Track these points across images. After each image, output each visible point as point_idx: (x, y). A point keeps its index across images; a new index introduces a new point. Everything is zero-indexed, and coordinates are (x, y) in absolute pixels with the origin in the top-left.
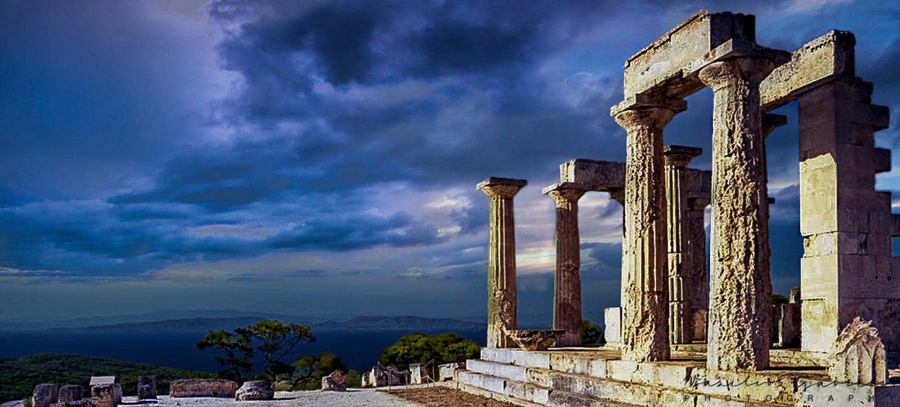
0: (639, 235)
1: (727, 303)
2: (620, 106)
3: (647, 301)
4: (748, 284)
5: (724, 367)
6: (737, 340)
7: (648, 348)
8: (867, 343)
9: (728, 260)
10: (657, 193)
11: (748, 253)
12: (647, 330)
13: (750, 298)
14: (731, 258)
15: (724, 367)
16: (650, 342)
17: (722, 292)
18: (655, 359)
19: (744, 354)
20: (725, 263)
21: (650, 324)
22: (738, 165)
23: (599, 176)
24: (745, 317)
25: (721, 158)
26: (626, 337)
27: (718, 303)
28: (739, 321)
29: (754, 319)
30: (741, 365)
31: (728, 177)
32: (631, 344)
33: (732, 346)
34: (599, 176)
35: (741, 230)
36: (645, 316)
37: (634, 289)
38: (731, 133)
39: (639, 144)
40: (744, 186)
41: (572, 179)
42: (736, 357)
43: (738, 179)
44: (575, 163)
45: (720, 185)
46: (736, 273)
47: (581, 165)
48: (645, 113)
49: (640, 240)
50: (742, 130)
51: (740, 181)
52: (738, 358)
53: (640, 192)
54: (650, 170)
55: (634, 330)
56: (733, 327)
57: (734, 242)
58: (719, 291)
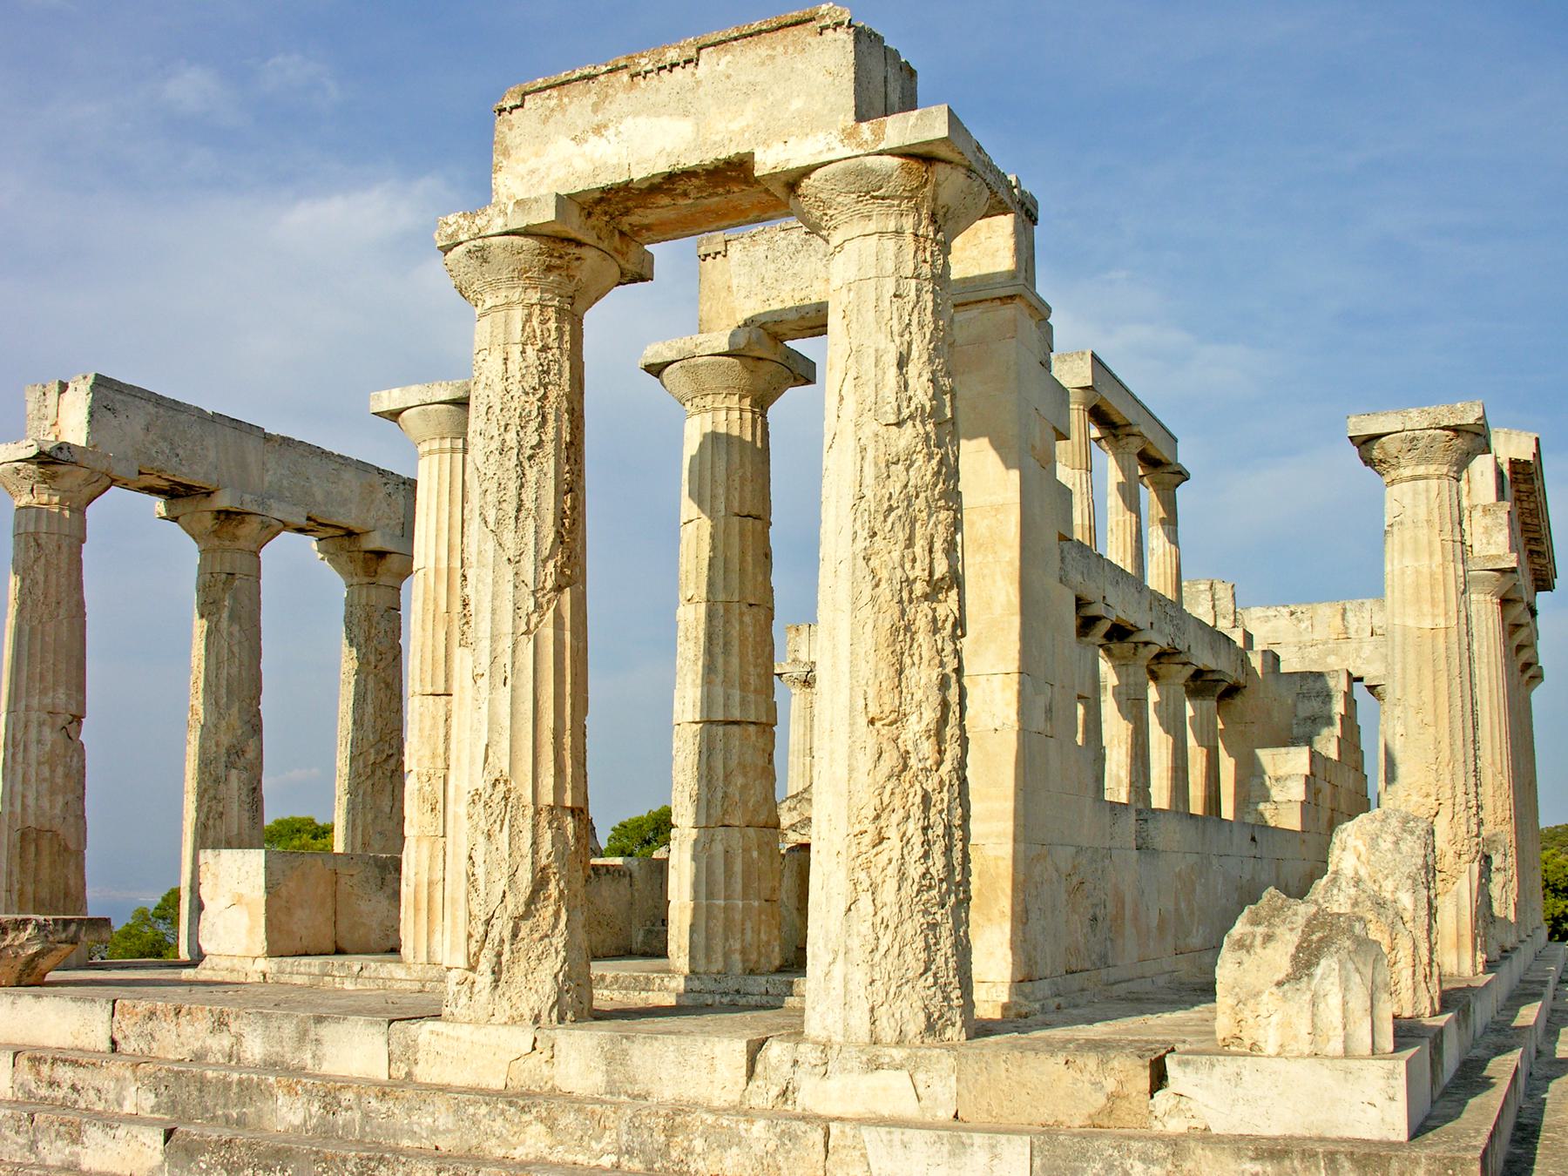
1: (893, 845)
3: (547, 837)
4: (945, 795)
6: (923, 956)
7: (550, 978)
9: (891, 724)
10: (573, 508)
11: (945, 705)
12: (545, 927)
13: (951, 836)
14: (899, 718)
15: (887, 1032)
16: (553, 964)
17: (878, 817)
18: (569, 1015)
19: (939, 996)
20: (884, 731)
21: (551, 909)
22: (920, 456)
24: (940, 891)
25: (875, 427)
26: (474, 948)
27: (863, 849)
28: (928, 901)
29: (956, 896)
30: (930, 1027)
31: (895, 487)
33: (910, 974)
34: (154, 443)
36: (540, 883)
37: (506, 798)
38: (902, 362)
39: (529, 348)
40: (930, 516)
42: (919, 1003)
43: (917, 497)
46: (912, 762)
50: (930, 361)
51: (920, 503)
52: (926, 1006)
54: (558, 431)
55: (501, 928)
57: (907, 672)
58: (872, 814)
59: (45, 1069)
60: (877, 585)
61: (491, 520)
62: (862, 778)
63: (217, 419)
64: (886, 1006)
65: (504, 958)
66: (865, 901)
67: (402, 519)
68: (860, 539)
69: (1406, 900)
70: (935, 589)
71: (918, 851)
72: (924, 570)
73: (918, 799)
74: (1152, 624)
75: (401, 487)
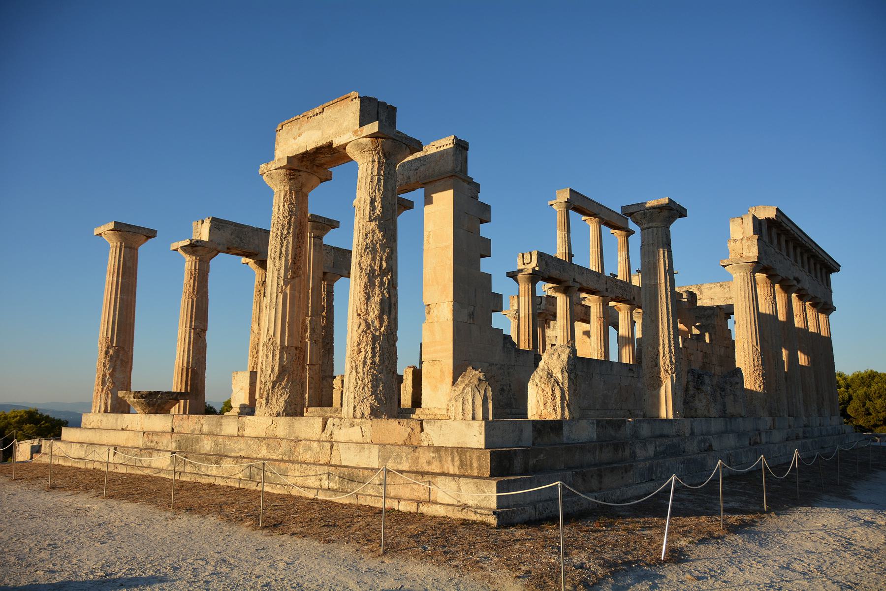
0: (280, 290)
2: (269, 166)
5: (359, 415)
8: (478, 385)
16: (286, 396)
17: (359, 344)
23: (234, 239)
31: (368, 241)
32: (266, 399)
34: (234, 239)
35: (377, 290)
37: (272, 344)
41: (205, 237)
42: (369, 405)
43: (377, 243)
44: (211, 222)
45: (360, 246)
47: (217, 224)
48: (293, 175)
49: (281, 297)
53: (284, 249)
55: (269, 385)
56: (367, 377)
58: (356, 344)
59: (150, 436)
60: (362, 272)
61: (273, 258)
62: (355, 332)
63: (259, 230)
64: (359, 406)
65: (270, 395)
66: (354, 371)
67: (333, 261)
68: (358, 257)
69: (559, 376)
70: (383, 273)
71: (370, 355)
72: (378, 267)
73: (370, 339)
74: (607, 289)
75: (333, 250)
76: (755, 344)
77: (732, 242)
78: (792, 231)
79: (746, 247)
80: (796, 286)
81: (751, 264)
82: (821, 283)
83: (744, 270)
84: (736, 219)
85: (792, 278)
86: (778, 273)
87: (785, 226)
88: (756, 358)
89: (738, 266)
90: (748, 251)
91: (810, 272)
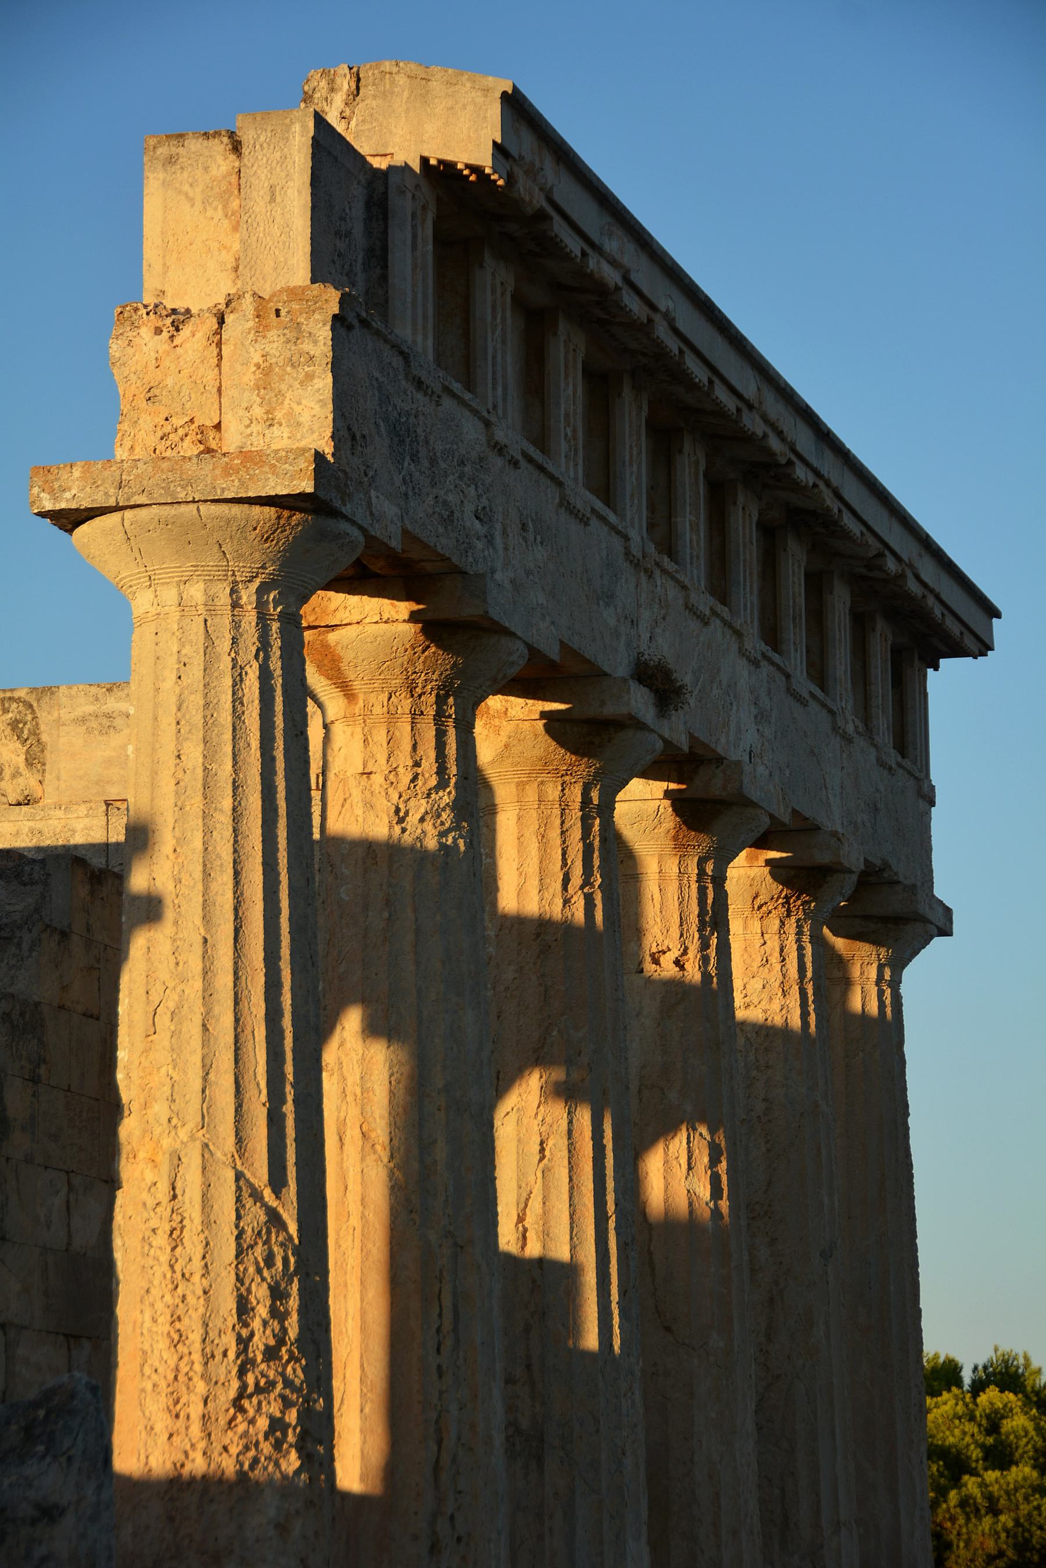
76: (259, 1173)
77: (146, 332)
78: (631, 302)
79: (250, 377)
80: (640, 726)
81: (270, 512)
82: (851, 724)
83: (212, 559)
84: (194, 145)
85: (620, 666)
86: (495, 613)
87: (574, 245)
88: (260, 1293)
89: (164, 522)
90: (258, 411)
91: (772, 636)
